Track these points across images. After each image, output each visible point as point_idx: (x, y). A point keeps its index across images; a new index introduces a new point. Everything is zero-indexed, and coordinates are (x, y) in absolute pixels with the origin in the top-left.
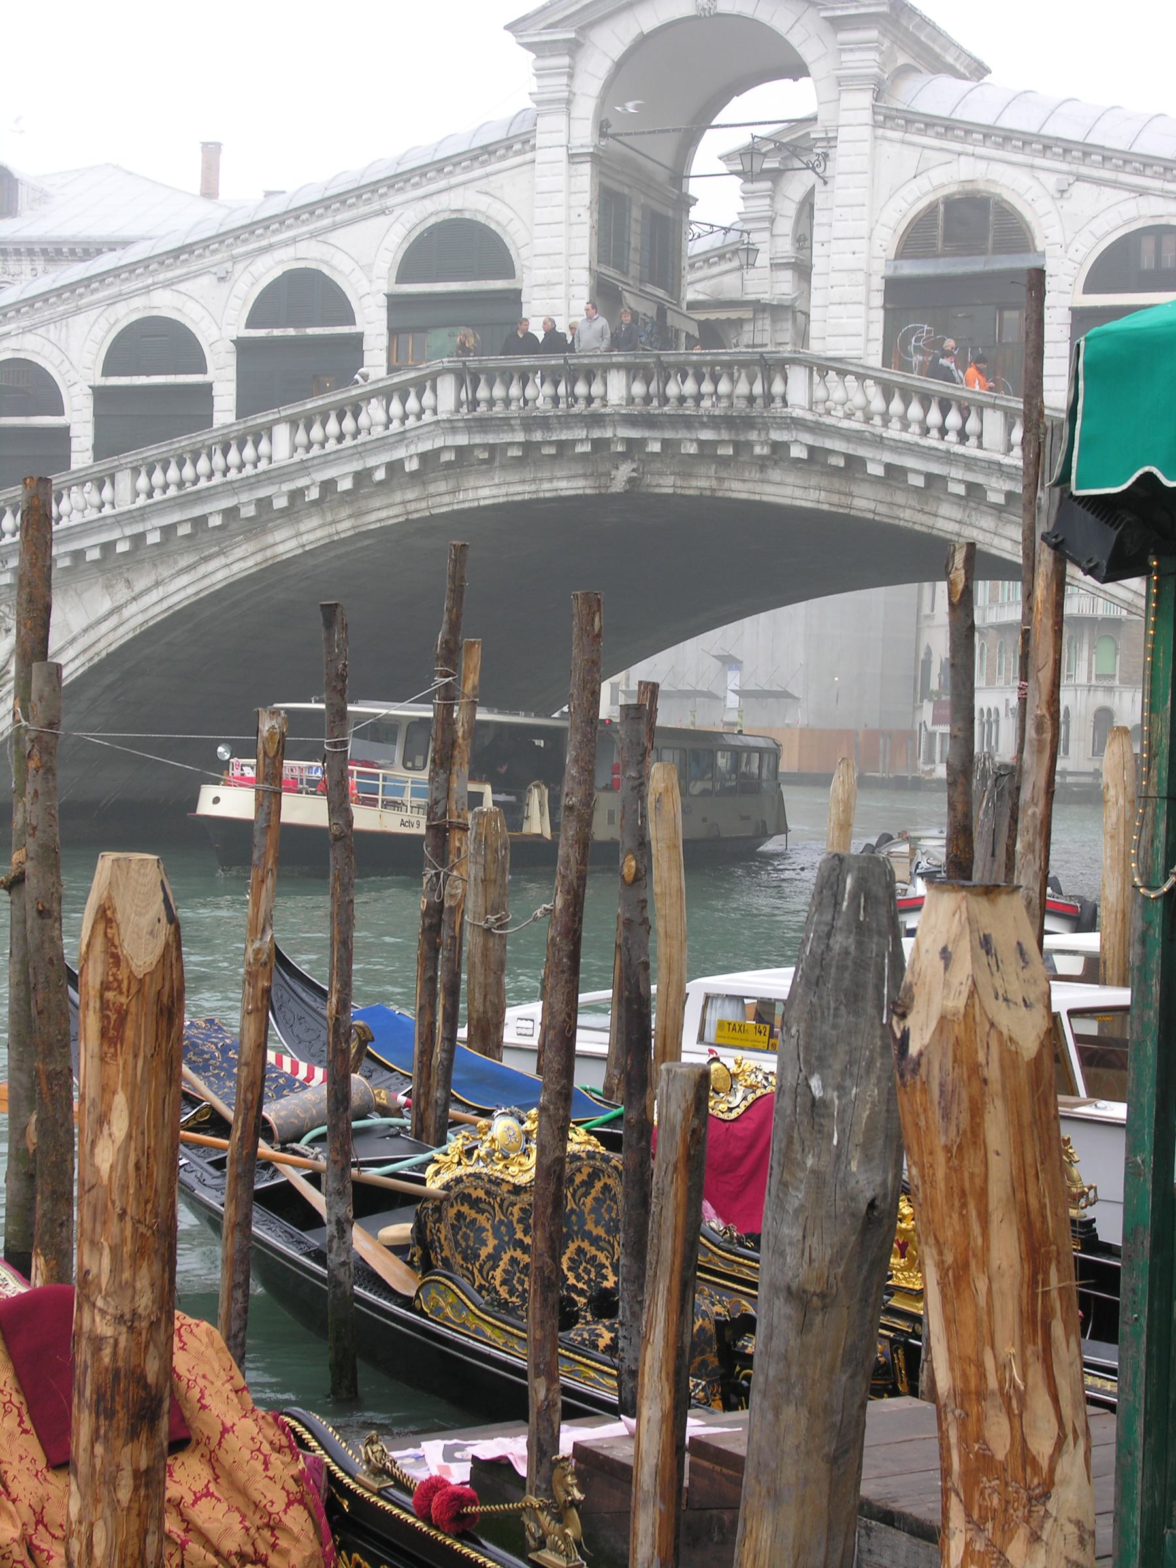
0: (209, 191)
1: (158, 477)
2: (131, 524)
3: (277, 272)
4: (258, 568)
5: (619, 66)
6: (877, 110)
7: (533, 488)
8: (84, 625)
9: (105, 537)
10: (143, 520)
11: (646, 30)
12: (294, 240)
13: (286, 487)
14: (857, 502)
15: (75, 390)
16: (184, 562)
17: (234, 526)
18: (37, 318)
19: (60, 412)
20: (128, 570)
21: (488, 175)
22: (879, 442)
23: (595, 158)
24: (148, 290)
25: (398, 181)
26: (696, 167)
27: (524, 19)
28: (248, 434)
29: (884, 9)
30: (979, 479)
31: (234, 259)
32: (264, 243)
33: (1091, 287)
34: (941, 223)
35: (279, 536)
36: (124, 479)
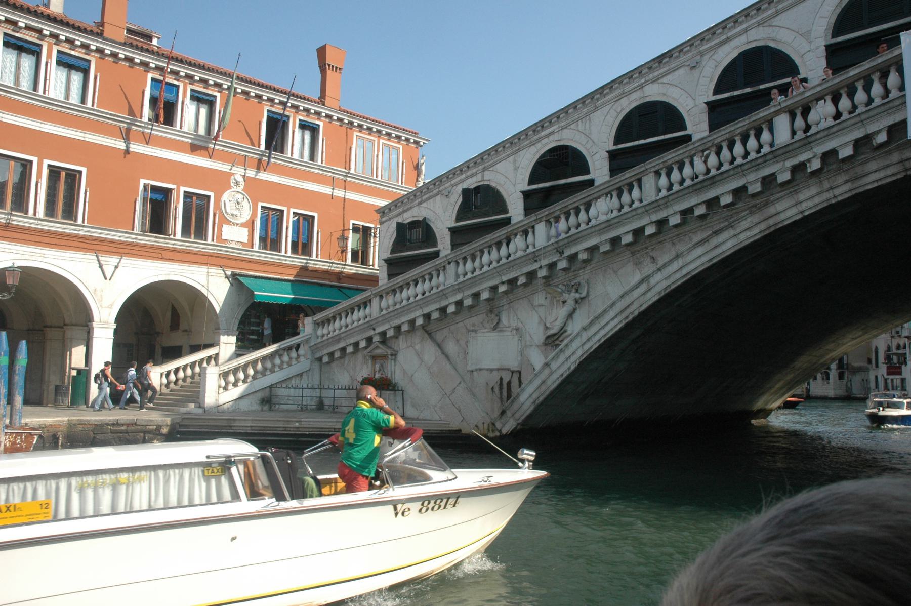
2: (656, 212)
3: (735, 54)
4: (763, 235)
8: (621, 293)
9: (636, 225)
10: (667, 207)
12: (746, 31)
13: (789, 163)
15: (597, 157)
16: (697, 238)
19: (588, 172)
20: (653, 249)
24: (641, 87)
28: (750, 129)
31: (702, 54)
32: (723, 38)
35: (780, 206)
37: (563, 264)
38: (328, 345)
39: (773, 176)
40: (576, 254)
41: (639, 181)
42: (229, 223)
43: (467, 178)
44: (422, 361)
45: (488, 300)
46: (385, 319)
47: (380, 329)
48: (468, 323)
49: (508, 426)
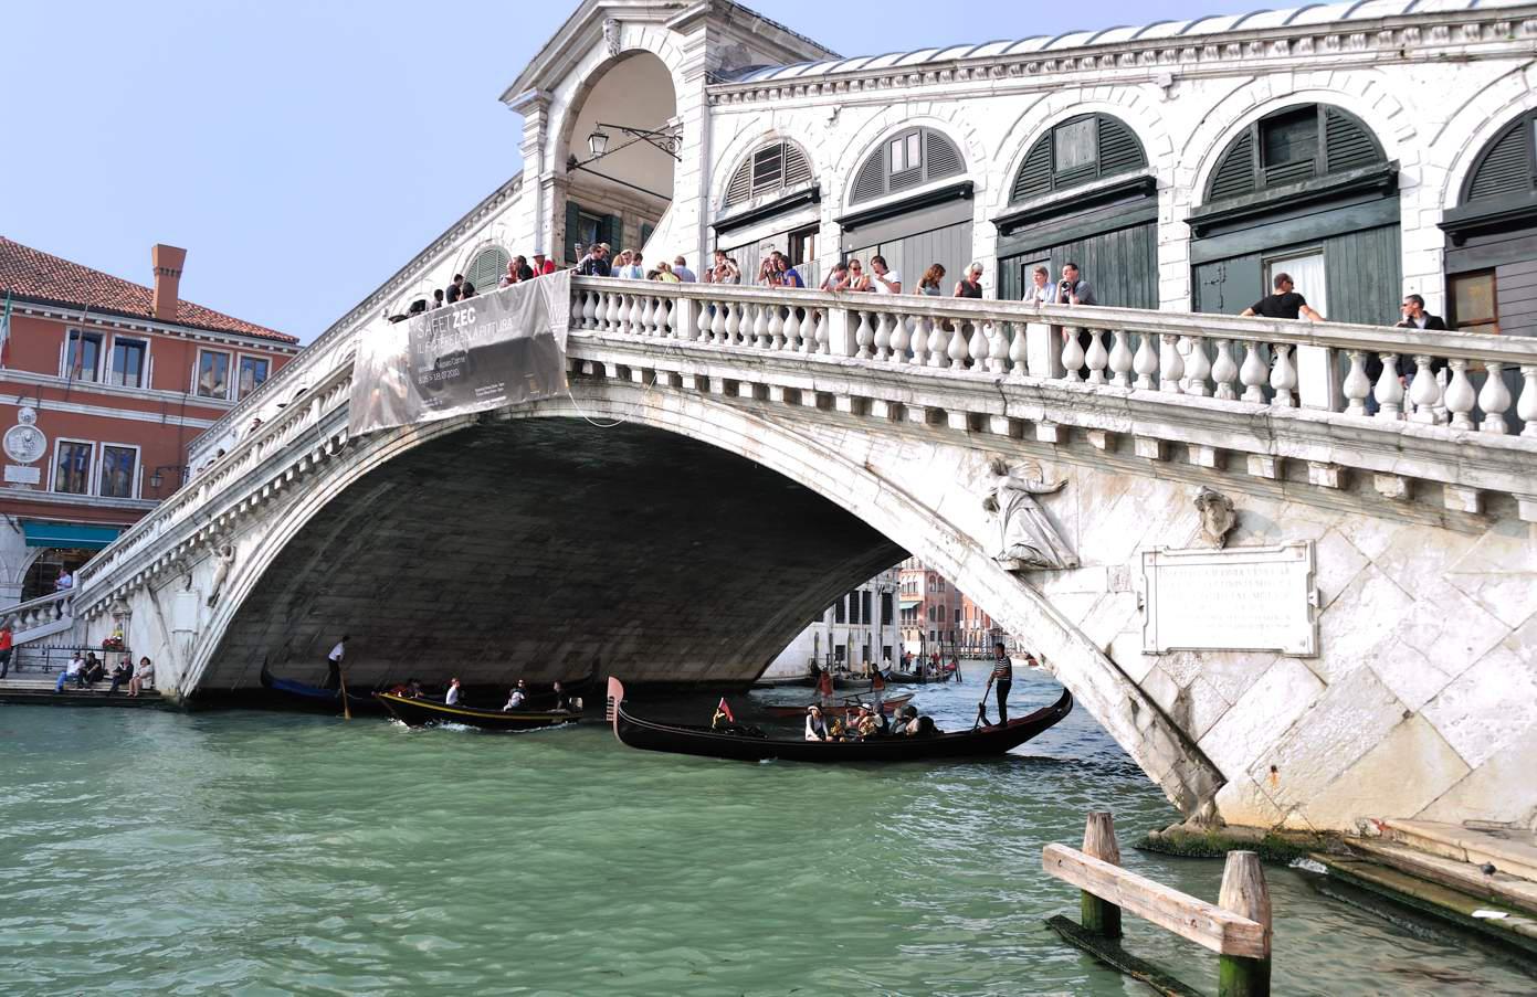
5: (575, 111)
6: (710, 91)
7: (436, 427)
12: (415, 282)
13: (317, 445)
14: (615, 407)
18: (314, 359)
21: (503, 211)
22: (603, 345)
23: (557, 182)
24: (354, 331)
25: (459, 227)
27: (510, 90)
29: (702, 7)
30: (675, 366)
31: (390, 302)
33: (856, 196)
34: (752, 172)
36: (255, 449)
38: (85, 602)
42: (14, 463)
44: (145, 622)
46: (117, 574)
47: (116, 587)
49: (188, 688)
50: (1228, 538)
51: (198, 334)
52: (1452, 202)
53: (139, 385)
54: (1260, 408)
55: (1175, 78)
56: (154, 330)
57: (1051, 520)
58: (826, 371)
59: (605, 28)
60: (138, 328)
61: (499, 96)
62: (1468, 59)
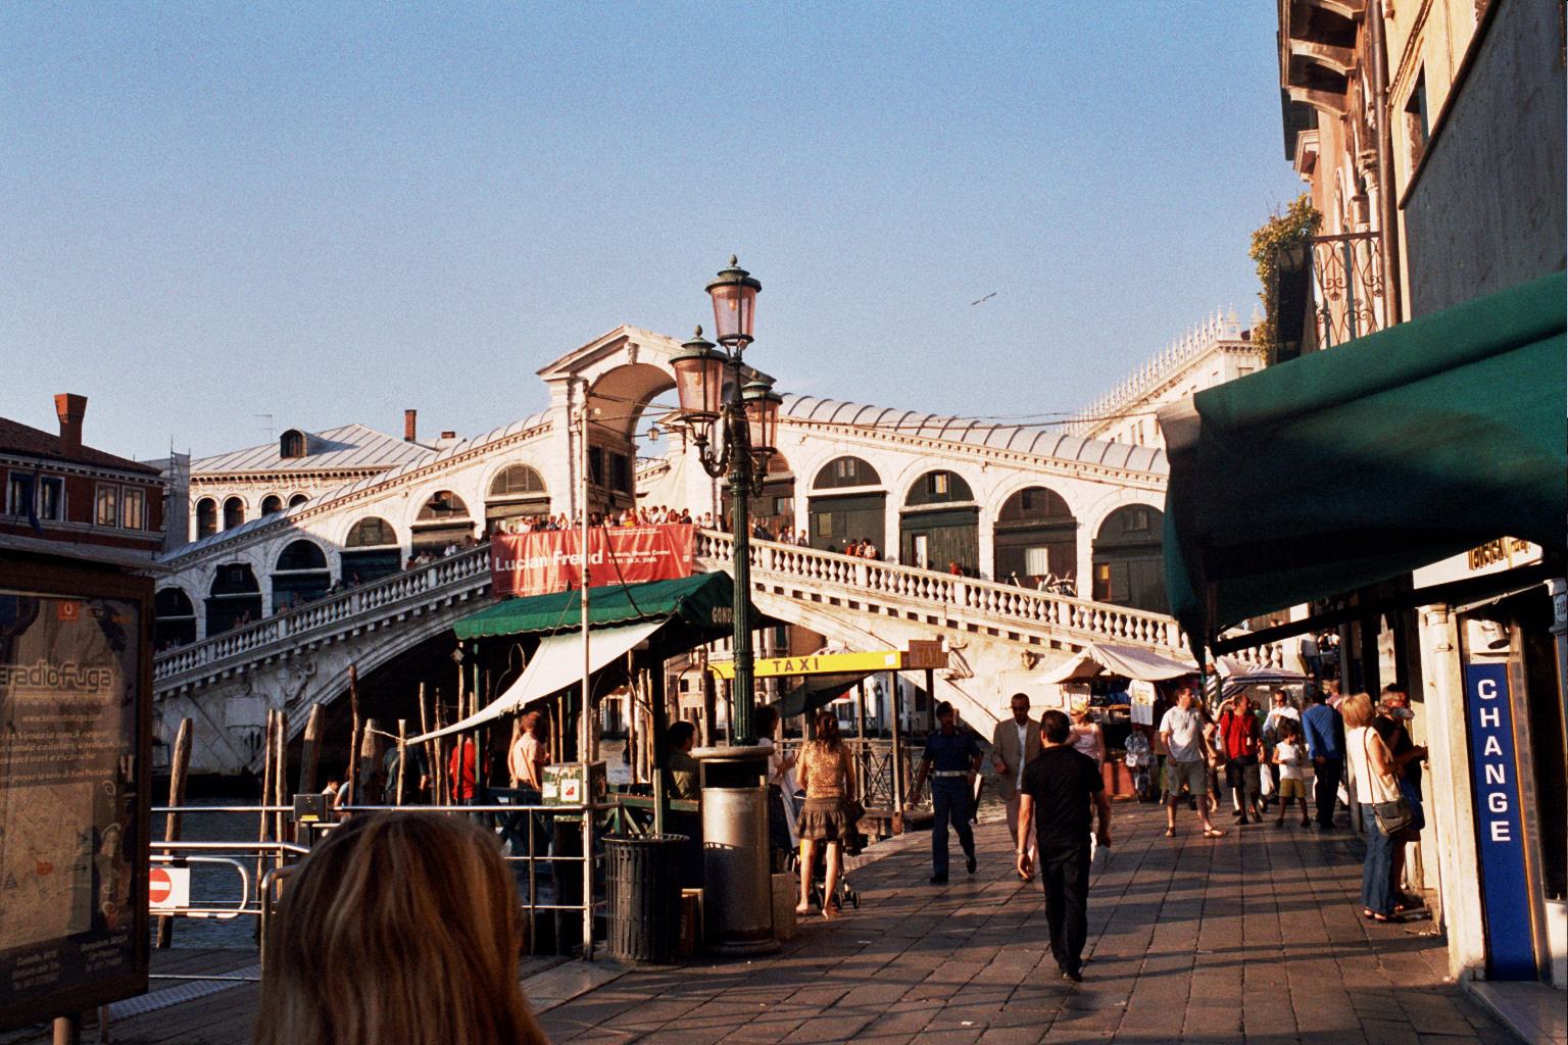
0: (410, 438)
1: (372, 598)
9: (347, 629)
11: (604, 372)
12: (438, 477)
13: (436, 600)
16: (386, 639)
17: (410, 619)
19: (324, 565)
24: (366, 504)
26: (638, 432)
33: (816, 486)
35: (432, 624)
36: (355, 599)
37: (298, 652)
39: (427, 606)
40: (307, 645)
41: (350, 599)
43: (222, 556)
45: (242, 674)
48: (226, 690)
50: (1032, 667)
51: (99, 472)
52: (1095, 537)
53: (53, 516)
54: (1047, 624)
55: (987, 464)
56: (70, 470)
57: (962, 658)
58: (858, 593)
59: (626, 346)
60: (59, 469)
61: (539, 369)
62: (1100, 482)
